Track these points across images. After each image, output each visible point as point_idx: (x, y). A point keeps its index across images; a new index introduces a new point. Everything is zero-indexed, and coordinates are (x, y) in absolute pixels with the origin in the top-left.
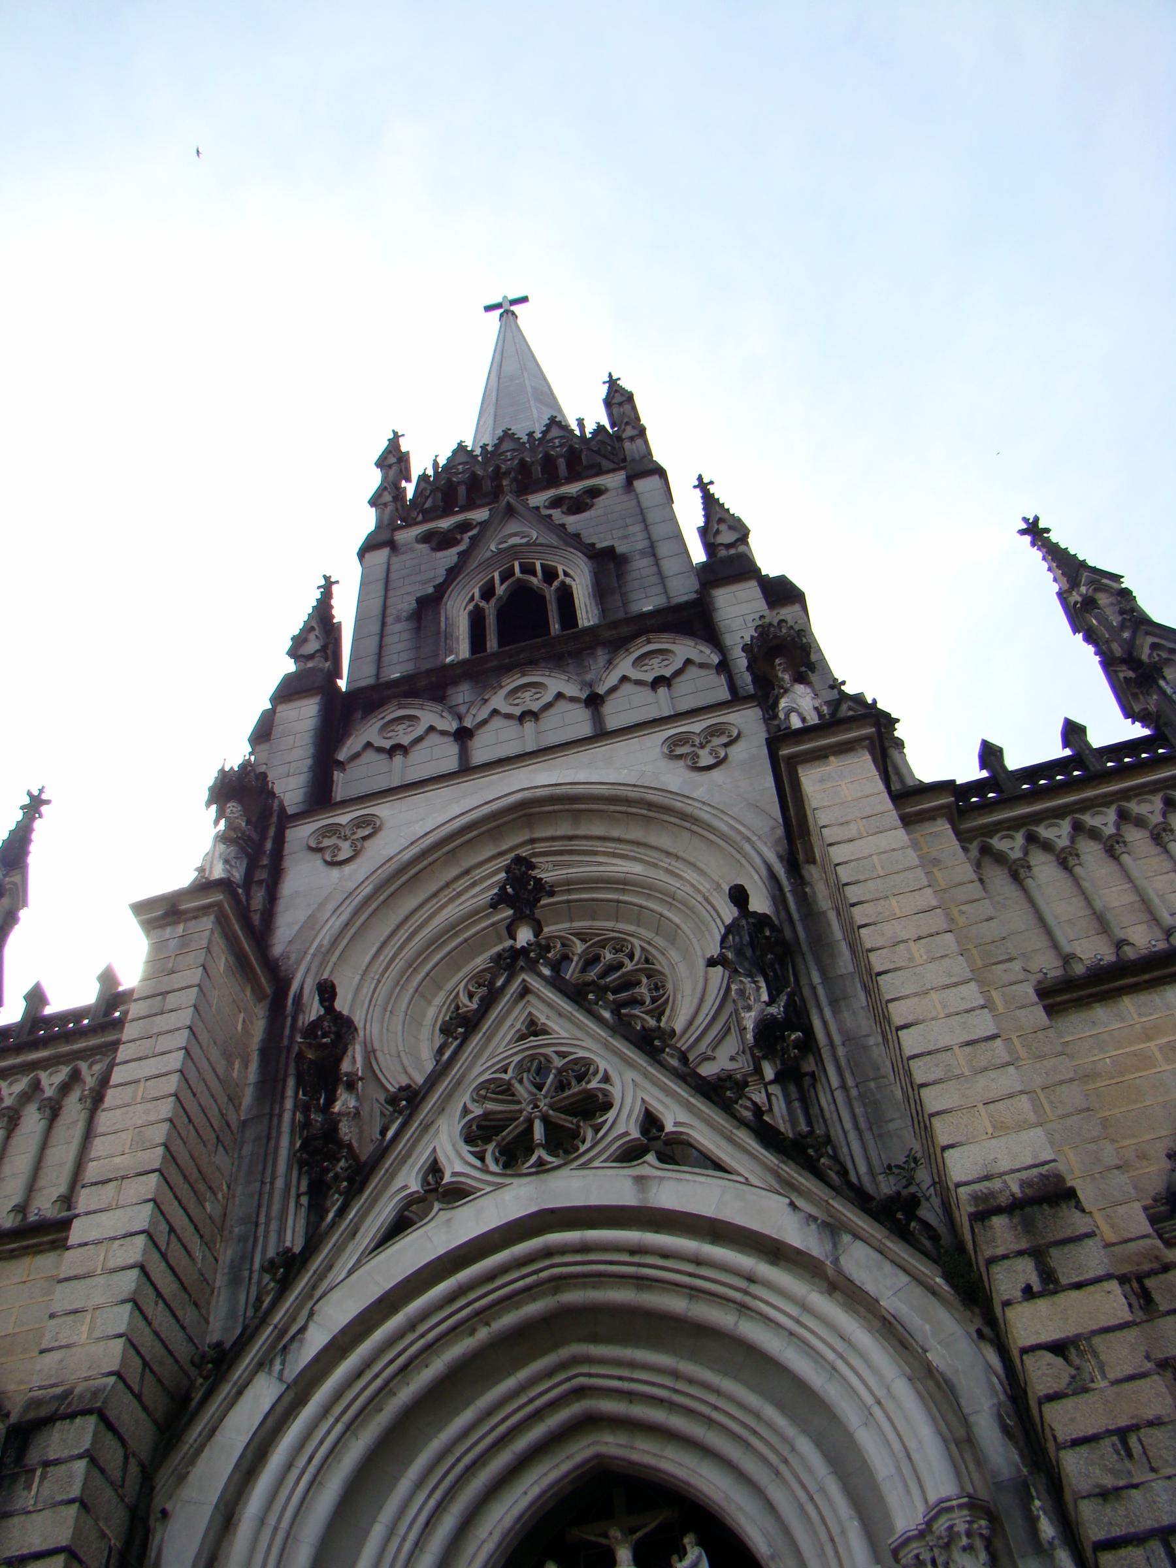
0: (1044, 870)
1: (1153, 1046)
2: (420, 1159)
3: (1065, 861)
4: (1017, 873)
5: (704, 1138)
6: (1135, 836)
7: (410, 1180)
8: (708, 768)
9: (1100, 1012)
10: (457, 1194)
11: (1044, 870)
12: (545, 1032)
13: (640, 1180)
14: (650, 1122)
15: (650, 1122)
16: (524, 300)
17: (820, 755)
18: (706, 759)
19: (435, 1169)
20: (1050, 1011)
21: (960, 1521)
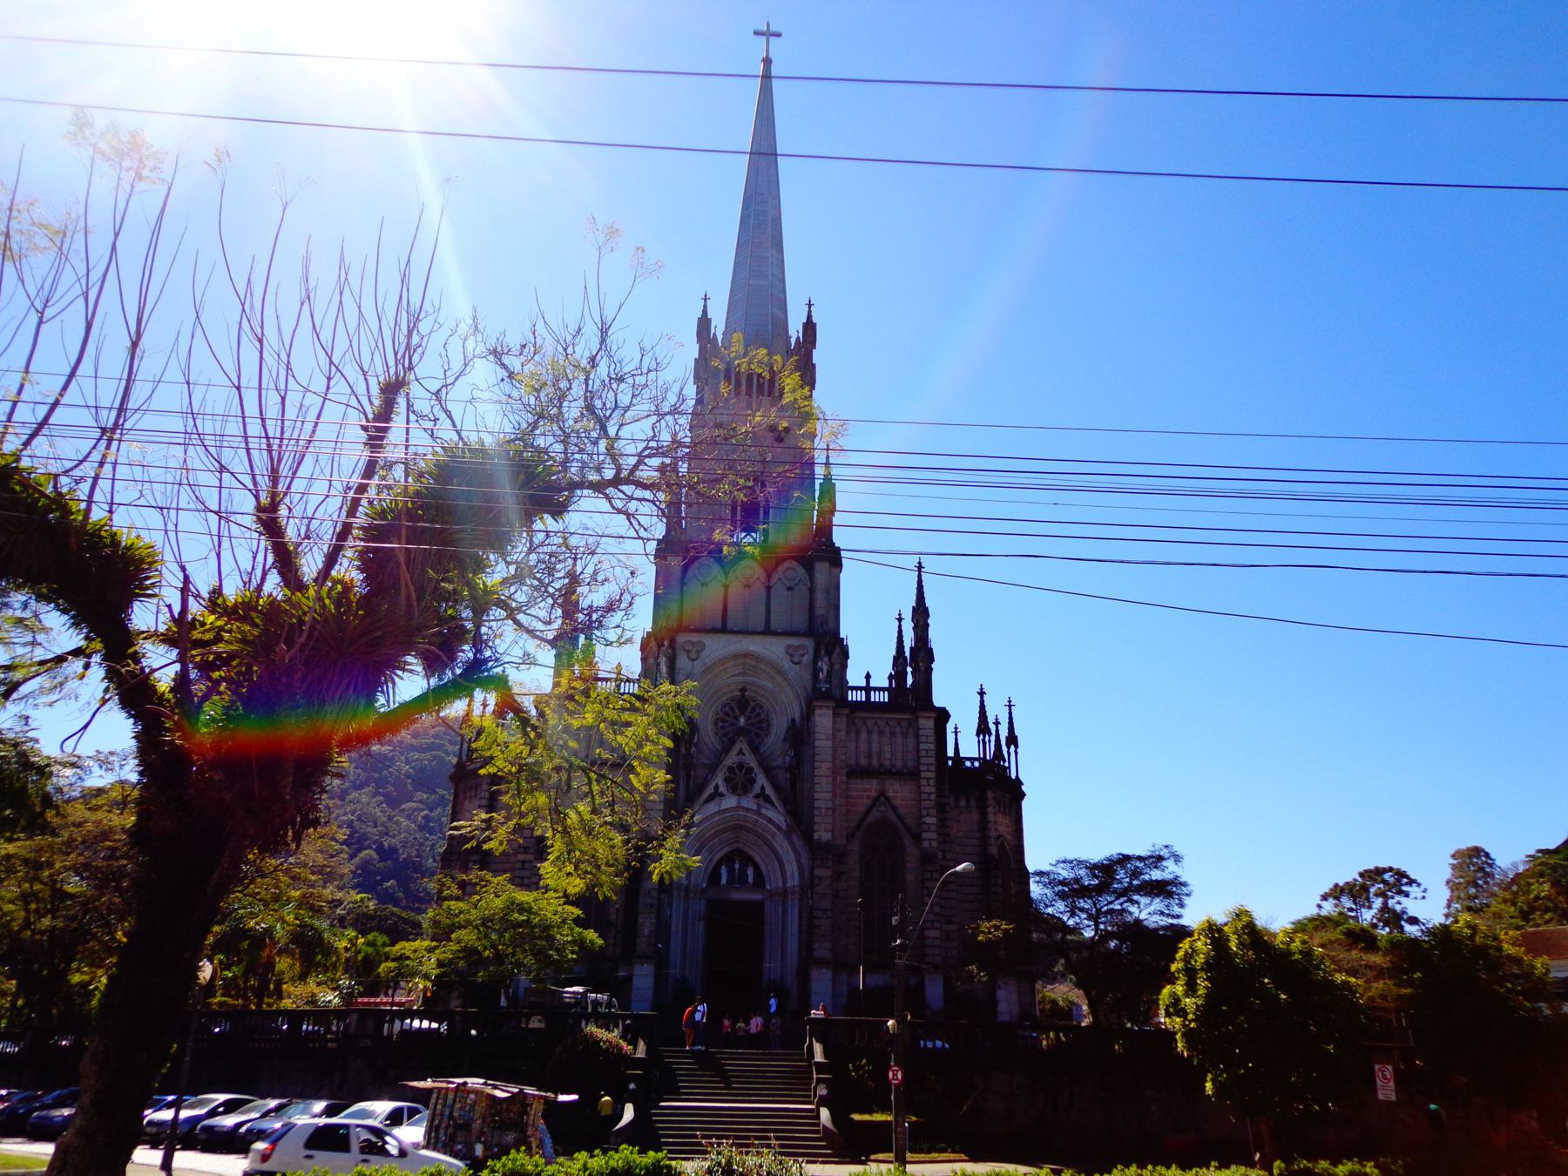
0: (864, 735)
1: (865, 794)
2: (713, 785)
3: (869, 732)
4: (858, 733)
5: (773, 798)
6: (887, 729)
7: (710, 790)
8: (796, 663)
9: (859, 781)
10: (722, 795)
11: (864, 735)
12: (744, 754)
13: (758, 805)
14: (763, 789)
15: (763, 789)
16: (779, 35)
17: (821, 707)
18: (796, 659)
19: (717, 787)
20: (848, 778)
21: (797, 889)
